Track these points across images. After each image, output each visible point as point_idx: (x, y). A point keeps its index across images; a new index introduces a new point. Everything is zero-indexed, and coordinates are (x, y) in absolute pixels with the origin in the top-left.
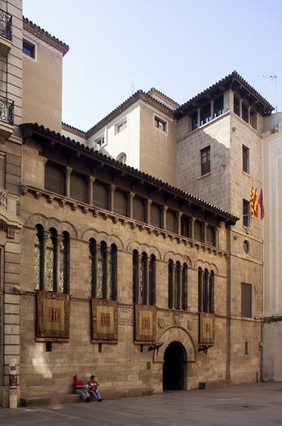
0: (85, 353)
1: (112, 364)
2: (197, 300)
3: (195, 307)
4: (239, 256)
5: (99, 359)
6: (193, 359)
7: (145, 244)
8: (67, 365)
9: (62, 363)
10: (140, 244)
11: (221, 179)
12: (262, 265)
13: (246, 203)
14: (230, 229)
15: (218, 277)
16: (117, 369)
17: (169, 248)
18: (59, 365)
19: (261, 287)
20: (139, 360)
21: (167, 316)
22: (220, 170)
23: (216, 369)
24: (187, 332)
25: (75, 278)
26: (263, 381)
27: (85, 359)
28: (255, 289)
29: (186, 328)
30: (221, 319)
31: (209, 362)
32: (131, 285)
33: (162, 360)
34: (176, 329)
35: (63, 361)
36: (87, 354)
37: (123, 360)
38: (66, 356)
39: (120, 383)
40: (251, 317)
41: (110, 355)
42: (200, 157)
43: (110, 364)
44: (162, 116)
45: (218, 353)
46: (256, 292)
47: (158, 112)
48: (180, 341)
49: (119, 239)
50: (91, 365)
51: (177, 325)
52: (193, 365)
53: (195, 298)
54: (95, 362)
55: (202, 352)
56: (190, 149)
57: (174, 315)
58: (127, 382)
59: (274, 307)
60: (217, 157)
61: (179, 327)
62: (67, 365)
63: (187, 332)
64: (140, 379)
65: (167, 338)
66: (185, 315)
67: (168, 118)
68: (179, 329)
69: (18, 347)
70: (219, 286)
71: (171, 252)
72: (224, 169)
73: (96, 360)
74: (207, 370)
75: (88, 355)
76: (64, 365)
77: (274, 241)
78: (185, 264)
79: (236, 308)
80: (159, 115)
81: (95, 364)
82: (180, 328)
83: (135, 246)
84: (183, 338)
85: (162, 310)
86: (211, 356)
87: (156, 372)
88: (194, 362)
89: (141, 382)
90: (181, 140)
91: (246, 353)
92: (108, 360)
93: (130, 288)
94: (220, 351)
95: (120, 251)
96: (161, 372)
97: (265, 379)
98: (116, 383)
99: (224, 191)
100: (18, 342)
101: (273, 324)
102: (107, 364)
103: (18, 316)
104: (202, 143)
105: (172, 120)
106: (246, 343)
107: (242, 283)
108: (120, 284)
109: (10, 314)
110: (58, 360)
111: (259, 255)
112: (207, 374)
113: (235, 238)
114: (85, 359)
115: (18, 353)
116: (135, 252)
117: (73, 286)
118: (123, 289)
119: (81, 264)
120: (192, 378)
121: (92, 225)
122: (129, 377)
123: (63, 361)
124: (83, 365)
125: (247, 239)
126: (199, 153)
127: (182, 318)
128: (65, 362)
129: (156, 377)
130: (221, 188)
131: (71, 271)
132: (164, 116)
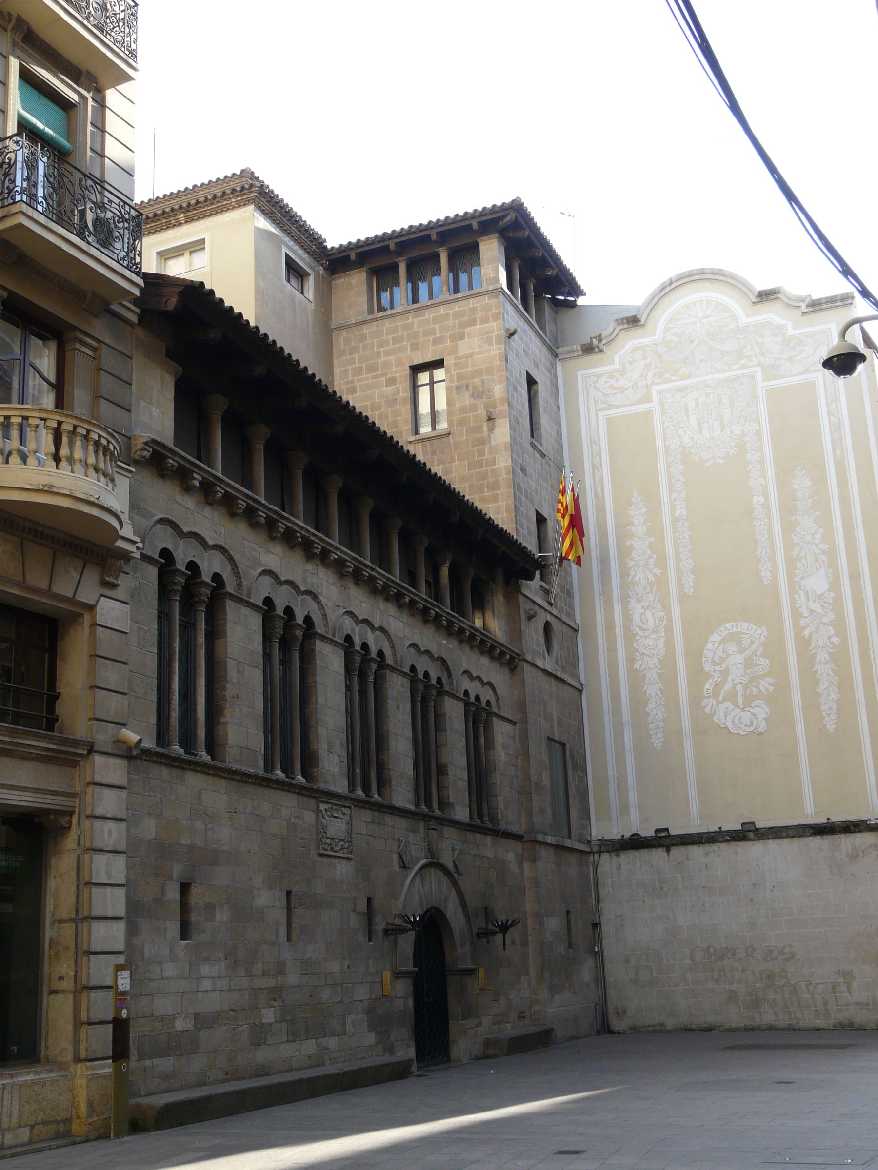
4: (539, 663)
8: (223, 984)
9: (213, 978)
11: (481, 453)
12: (580, 691)
13: (541, 520)
14: (518, 589)
18: (207, 984)
19: (582, 752)
22: (479, 429)
26: (611, 1032)
28: (572, 756)
33: (411, 968)
40: (570, 837)
42: (408, 384)
44: (302, 258)
46: (575, 769)
47: (291, 243)
49: (319, 602)
53: (462, 779)
55: (484, 940)
56: (378, 354)
59: (624, 809)
60: (468, 394)
67: (314, 263)
72: (491, 430)
77: (610, 627)
79: (542, 811)
80: (295, 252)
90: (349, 326)
91: (570, 945)
95: (323, 638)
97: (617, 1024)
99: (494, 486)
100: (121, 911)
101: (627, 859)
103: (123, 825)
104: (415, 347)
105: (322, 271)
106: (568, 912)
107: (548, 737)
109: (104, 818)
111: (572, 662)
113: (530, 618)
116: (349, 639)
125: (549, 618)
126: (408, 371)
130: (484, 476)
132: (305, 256)
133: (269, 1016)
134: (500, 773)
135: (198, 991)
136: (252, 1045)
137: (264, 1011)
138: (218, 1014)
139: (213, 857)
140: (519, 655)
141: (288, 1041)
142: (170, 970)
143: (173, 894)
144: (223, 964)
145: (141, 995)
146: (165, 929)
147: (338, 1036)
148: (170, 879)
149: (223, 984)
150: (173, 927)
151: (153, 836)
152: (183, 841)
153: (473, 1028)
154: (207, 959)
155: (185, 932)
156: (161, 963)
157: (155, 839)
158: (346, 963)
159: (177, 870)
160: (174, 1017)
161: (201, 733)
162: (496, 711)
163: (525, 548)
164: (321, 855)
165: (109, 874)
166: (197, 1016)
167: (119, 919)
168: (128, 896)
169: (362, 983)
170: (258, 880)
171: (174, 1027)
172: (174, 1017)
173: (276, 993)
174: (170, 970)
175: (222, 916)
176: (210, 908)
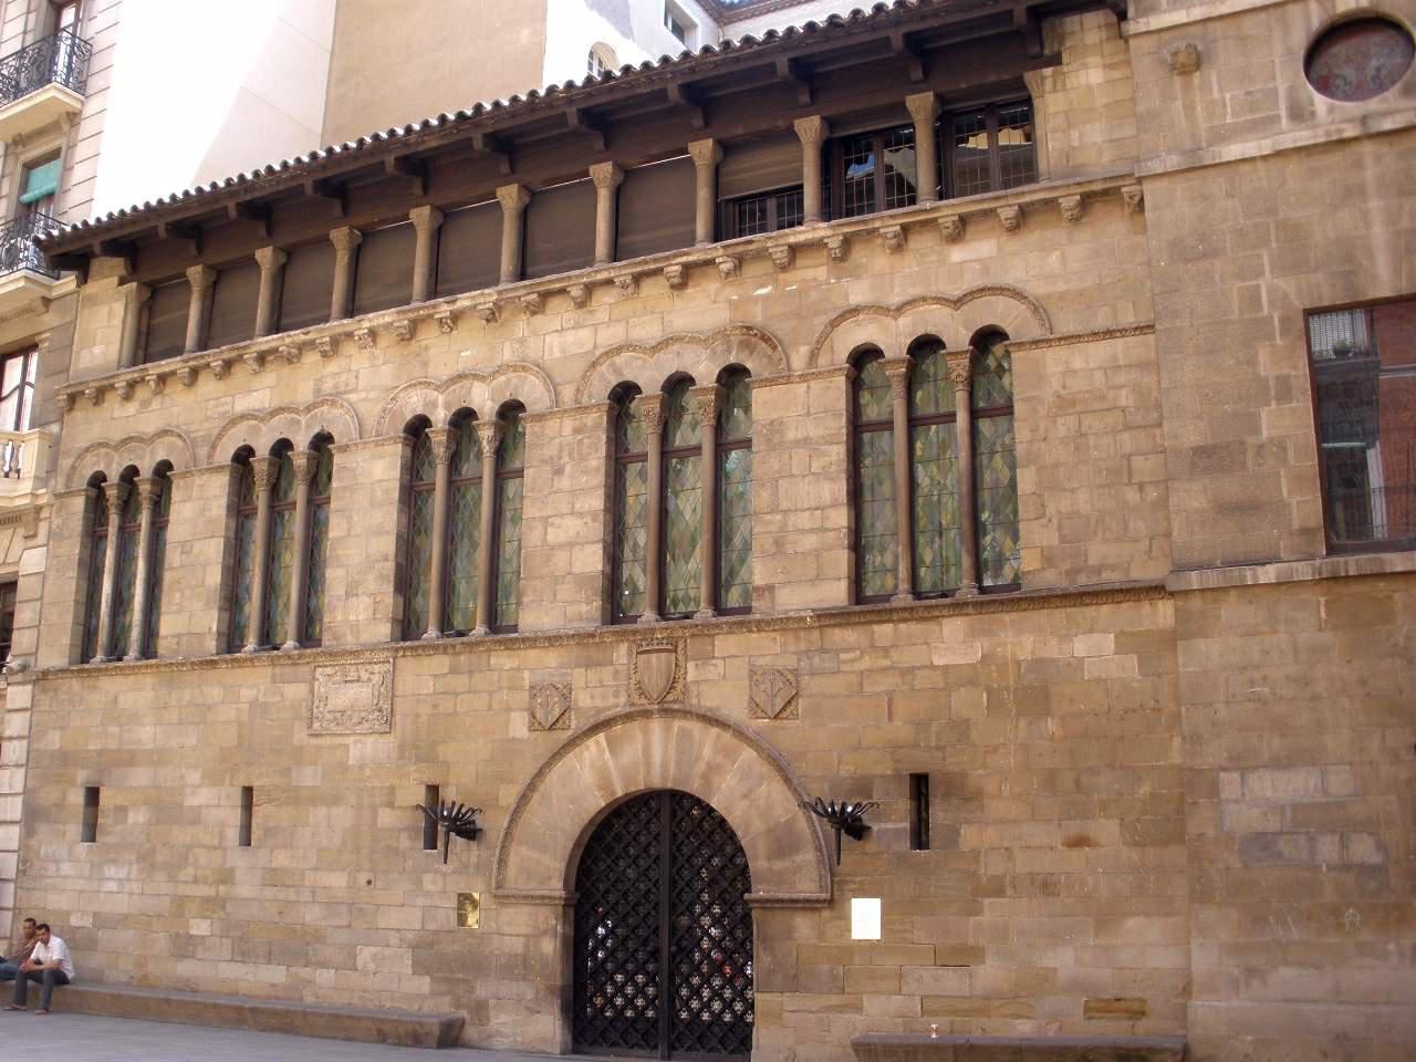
0: (189, 848)
1: (292, 896)
2: (843, 538)
3: (817, 578)
5: (239, 875)
6: (807, 887)
7: (461, 377)
8: (135, 887)
9: (120, 880)
10: (437, 388)
15: (1054, 360)
16: (312, 915)
17: (610, 335)
18: (112, 886)
20: (419, 882)
21: (587, 667)
23: (1063, 961)
24: (740, 733)
25: (178, 595)
27: (191, 871)
29: (737, 710)
30: (1105, 611)
31: (975, 910)
32: (389, 567)
33: (556, 887)
34: (656, 725)
35: (123, 873)
36: (197, 850)
37: (337, 881)
38: (133, 858)
39: (325, 977)
41: (282, 859)
43: (282, 895)
45: (1079, 842)
48: (694, 787)
50: (209, 891)
51: (668, 703)
52: (803, 925)
54: (223, 882)
57: (1060, 642)
58: (355, 975)
61: (667, 712)
62: (134, 886)
63: (740, 733)
64: (419, 967)
65: (588, 777)
66: (726, 644)
68: (677, 724)
69: (16, 830)
70: (1065, 404)
71: (618, 350)
73: (226, 877)
74: (963, 956)
75: (203, 857)
76: (127, 887)
78: (733, 377)
81: (222, 888)
82: (686, 714)
83: (414, 403)
84: (712, 770)
85: (553, 640)
86: (993, 867)
87: (517, 946)
88: (810, 905)
89: (424, 984)
92: (274, 878)
93: (382, 577)
94: (1106, 830)
96: (550, 947)
98: (304, 972)
100: (17, 814)
102: (269, 893)
108: (334, 578)
110: (111, 871)
112: (951, 982)
114: (191, 871)
115: (16, 848)
117: (168, 625)
118: (350, 593)
119: (197, 547)
120: (789, 1001)
121: (242, 405)
122: (365, 955)
123: (123, 873)
124: (183, 890)
127: (706, 658)
128: (129, 880)
129: (516, 968)
131: (168, 577)
133: (200, 927)
134: (1039, 469)
135: (99, 891)
136: (172, 955)
137: (192, 921)
138: (126, 917)
139: (129, 759)
140: (1130, 175)
141: (232, 960)
142: (66, 868)
143: (77, 798)
144: (135, 867)
145: (34, 889)
146: (64, 834)
147: (337, 970)
148: (73, 784)
149: (135, 887)
150: (75, 829)
151: (57, 747)
152: (91, 747)
153: (810, 1012)
154: (114, 861)
155: (91, 833)
156: (57, 862)
157: (60, 749)
158: (363, 878)
159: (83, 776)
160: (68, 913)
161: (135, 634)
162: (1037, 332)
163: (833, 21)
164: (311, 735)
165: (11, 786)
166: (96, 915)
167: (16, 822)
168: (24, 803)
169: (402, 905)
170: (194, 777)
171: (68, 920)
172: (68, 913)
173: (210, 905)
174: (66, 868)
175: (138, 817)
176: (122, 811)
